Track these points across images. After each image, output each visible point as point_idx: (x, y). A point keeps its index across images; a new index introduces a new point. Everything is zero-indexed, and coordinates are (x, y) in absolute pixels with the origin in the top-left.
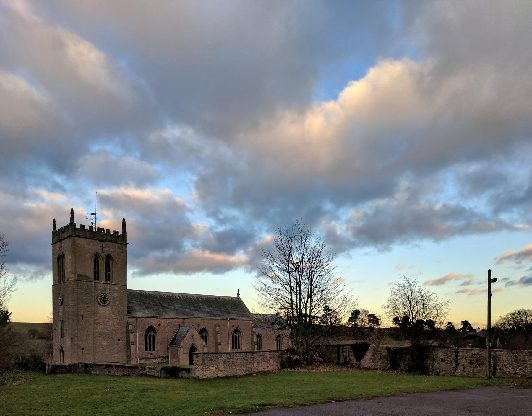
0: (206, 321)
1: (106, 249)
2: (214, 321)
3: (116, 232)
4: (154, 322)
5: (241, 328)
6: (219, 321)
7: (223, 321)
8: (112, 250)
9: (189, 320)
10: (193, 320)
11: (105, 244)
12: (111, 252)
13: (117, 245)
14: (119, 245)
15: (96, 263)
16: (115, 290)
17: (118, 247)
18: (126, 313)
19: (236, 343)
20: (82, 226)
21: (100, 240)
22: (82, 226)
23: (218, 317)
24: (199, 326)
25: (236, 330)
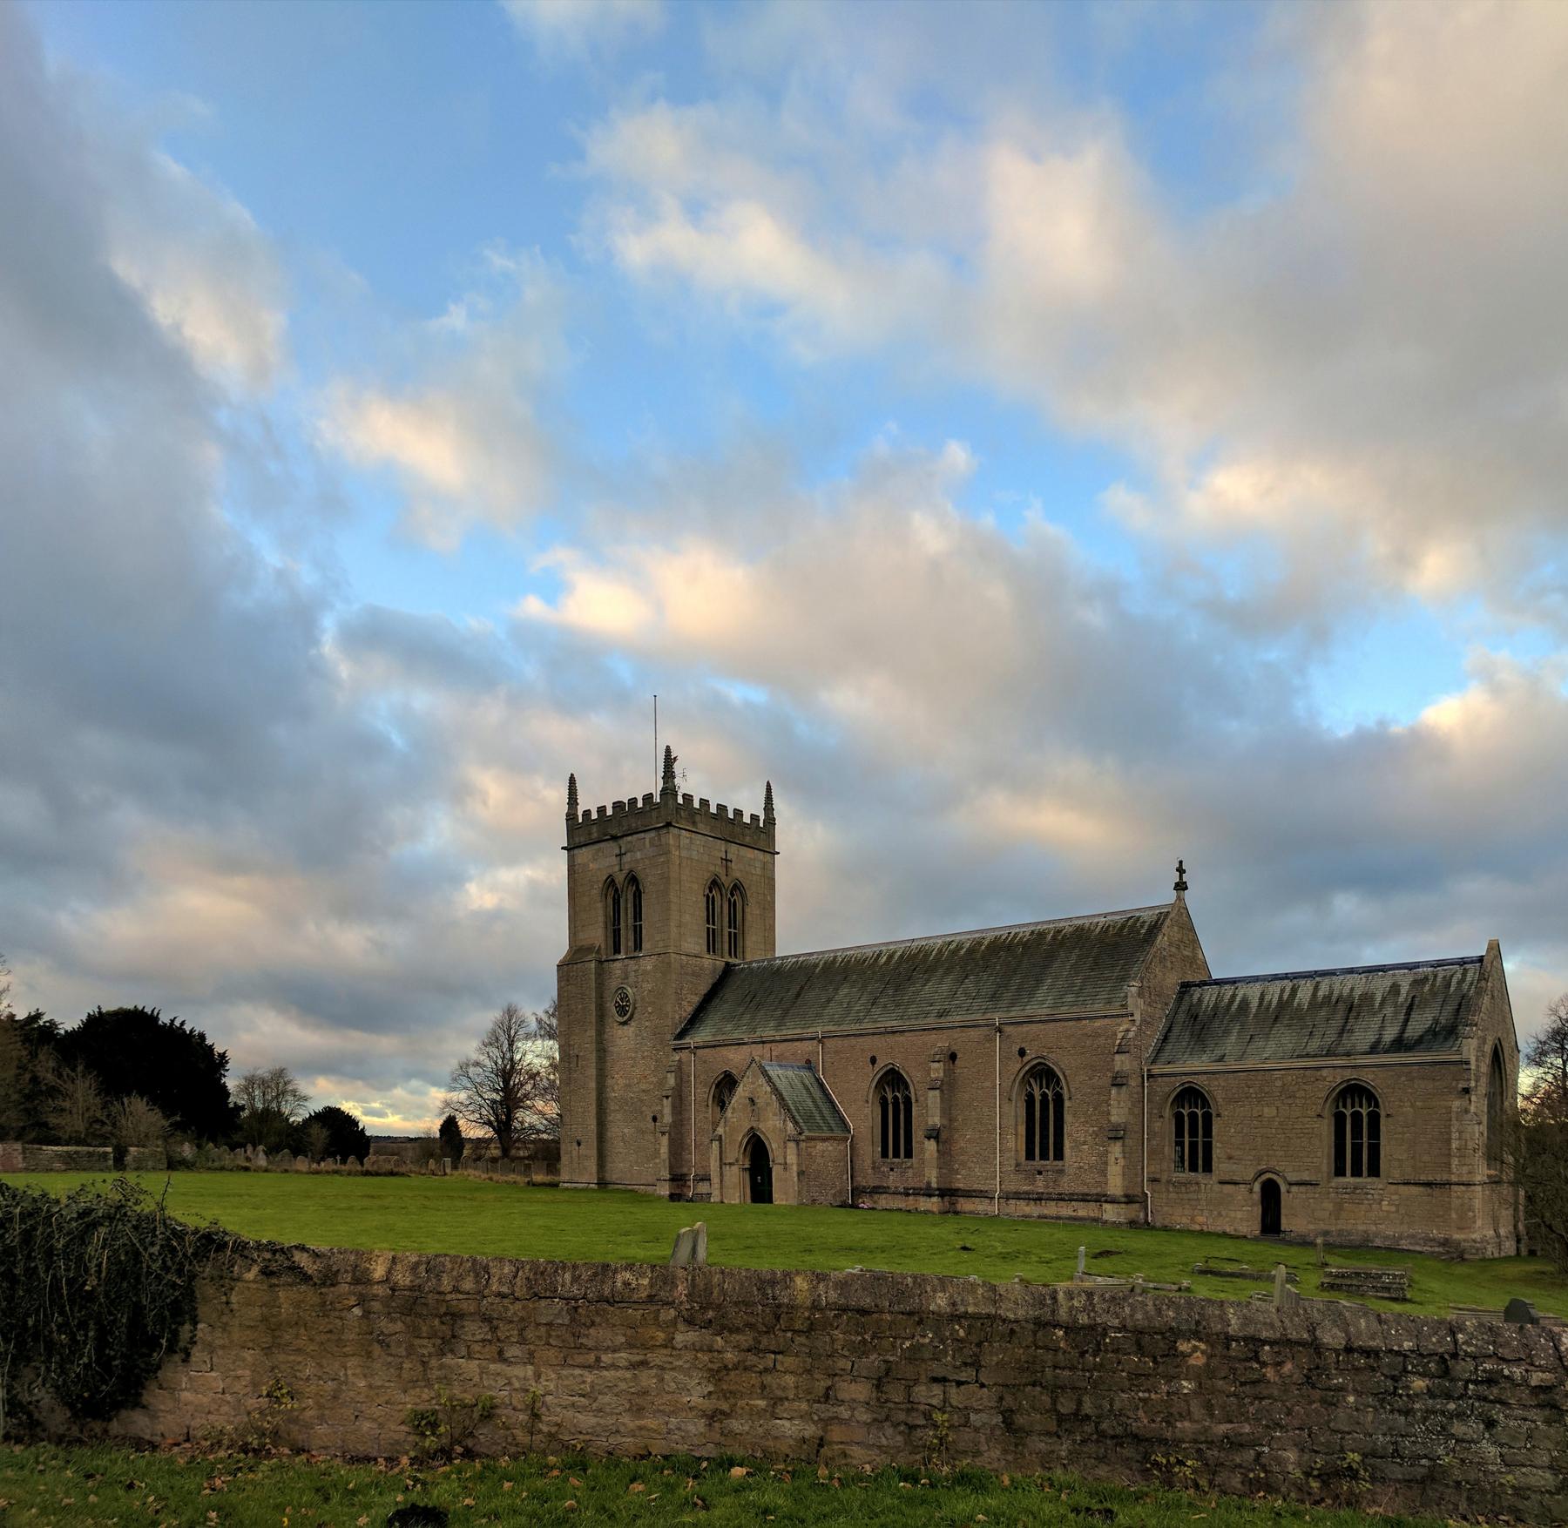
0: (900, 1038)
1: (626, 858)
2: (933, 1036)
3: (648, 798)
4: (734, 1058)
5: (1061, 1063)
6: (956, 1034)
7: (973, 1033)
8: (639, 855)
9: (838, 1042)
10: (853, 1041)
11: (623, 842)
12: (637, 861)
13: (648, 836)
14: (653, 834)
15: (616, 902)
16: (645, 973)
17: (651, 839)
18: (669, 1037)
19: (1044, 1132)
20: (587, 813)
21: (614, 838)
22: (587, 813)
23: (956, 1018)
24: (873, 1060)
25: (1043, 1073)
